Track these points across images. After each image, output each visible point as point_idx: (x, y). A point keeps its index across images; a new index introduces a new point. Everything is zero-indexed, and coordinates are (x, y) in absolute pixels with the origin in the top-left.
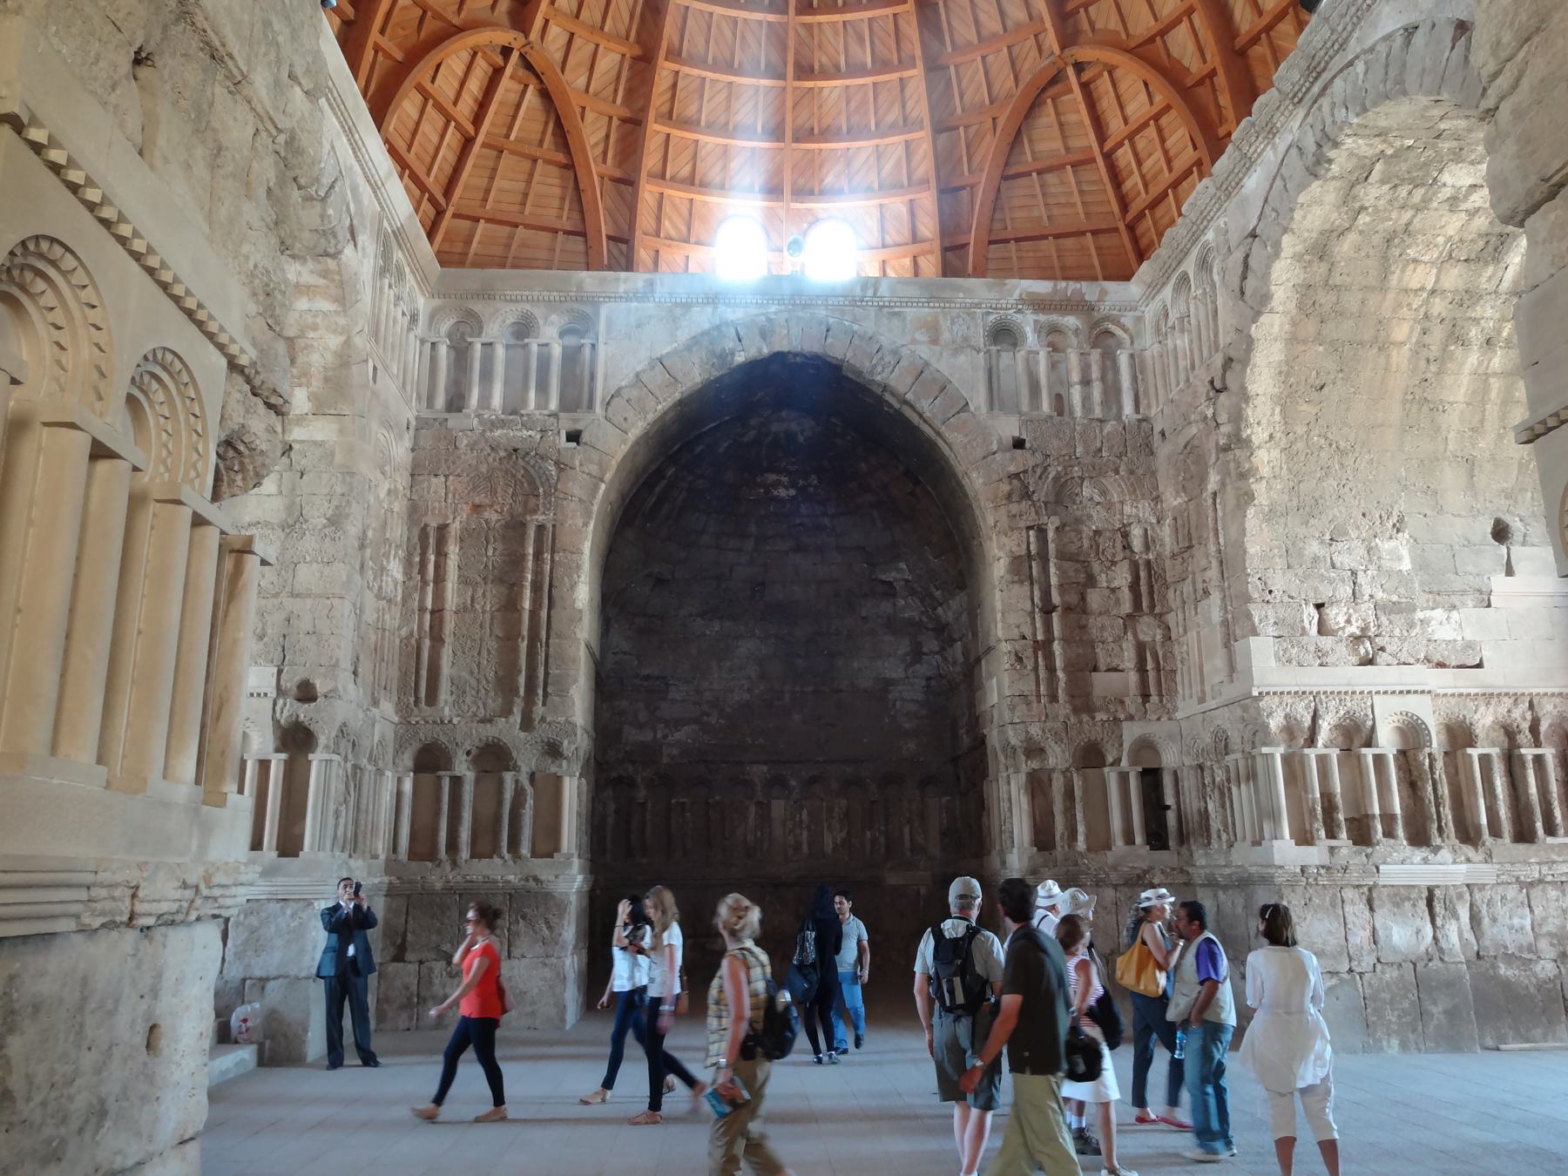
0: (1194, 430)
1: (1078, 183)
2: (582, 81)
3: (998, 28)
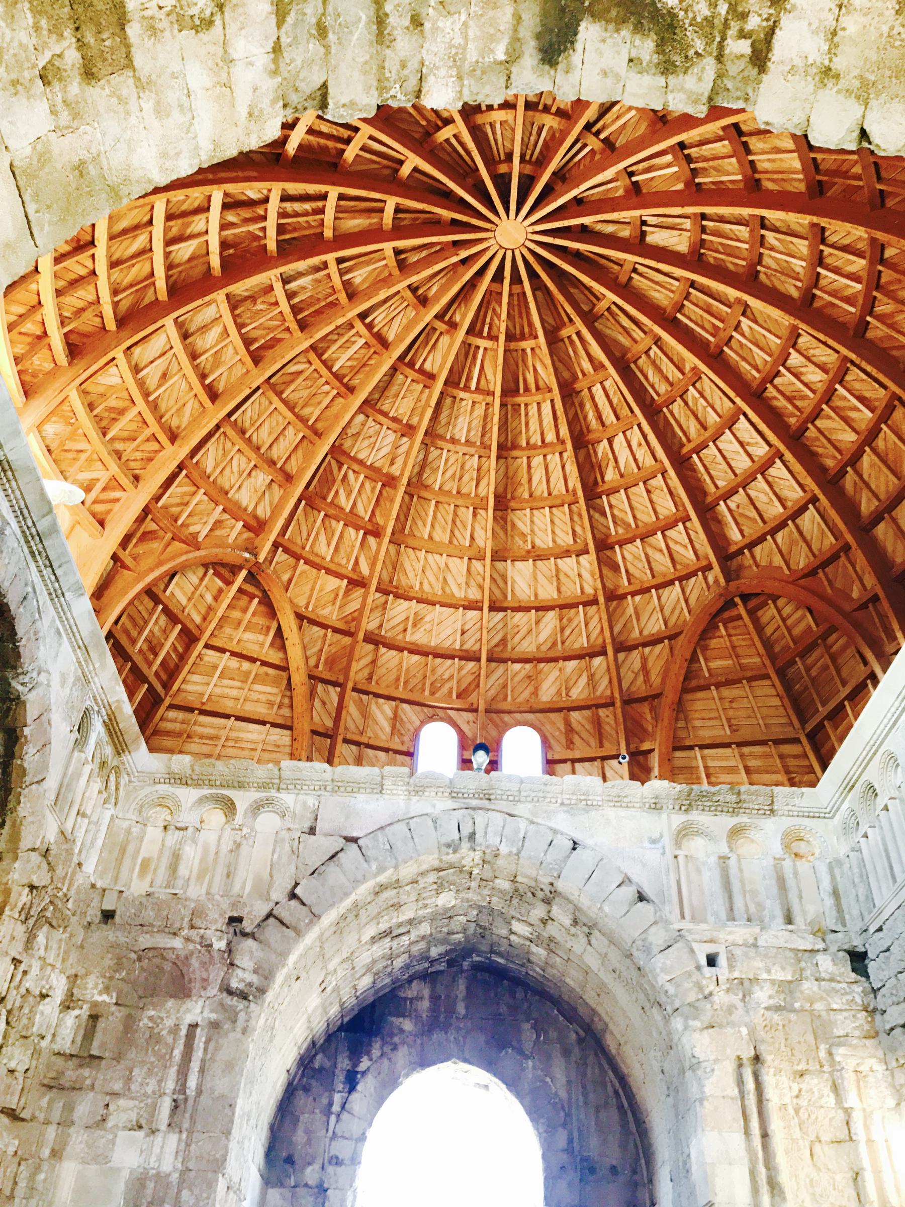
0: (177, 943)
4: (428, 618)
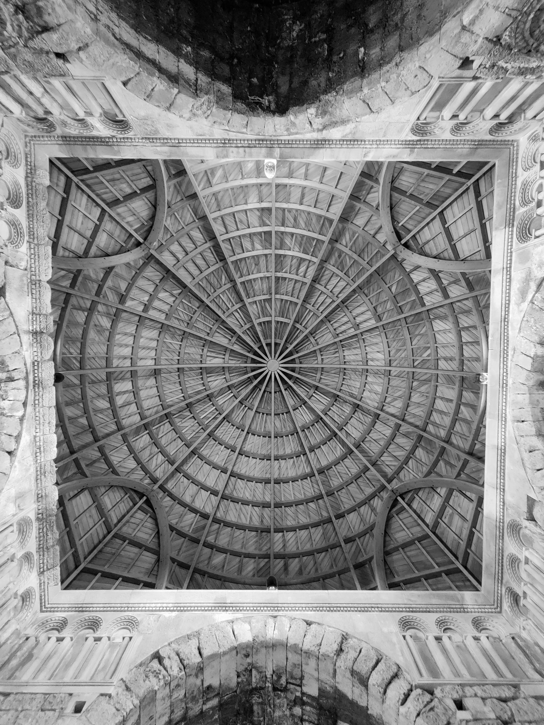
1: (112, 192)
2: (373, 218)
3: (181, 240)
4: (102, 338)
